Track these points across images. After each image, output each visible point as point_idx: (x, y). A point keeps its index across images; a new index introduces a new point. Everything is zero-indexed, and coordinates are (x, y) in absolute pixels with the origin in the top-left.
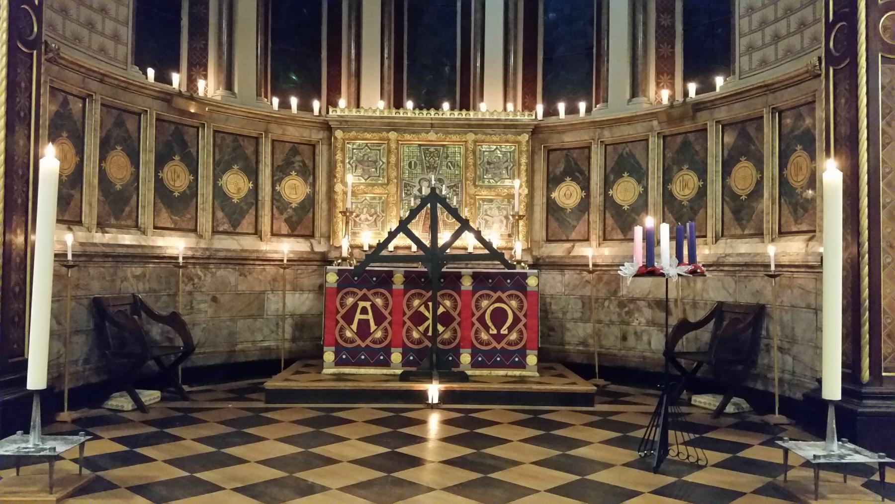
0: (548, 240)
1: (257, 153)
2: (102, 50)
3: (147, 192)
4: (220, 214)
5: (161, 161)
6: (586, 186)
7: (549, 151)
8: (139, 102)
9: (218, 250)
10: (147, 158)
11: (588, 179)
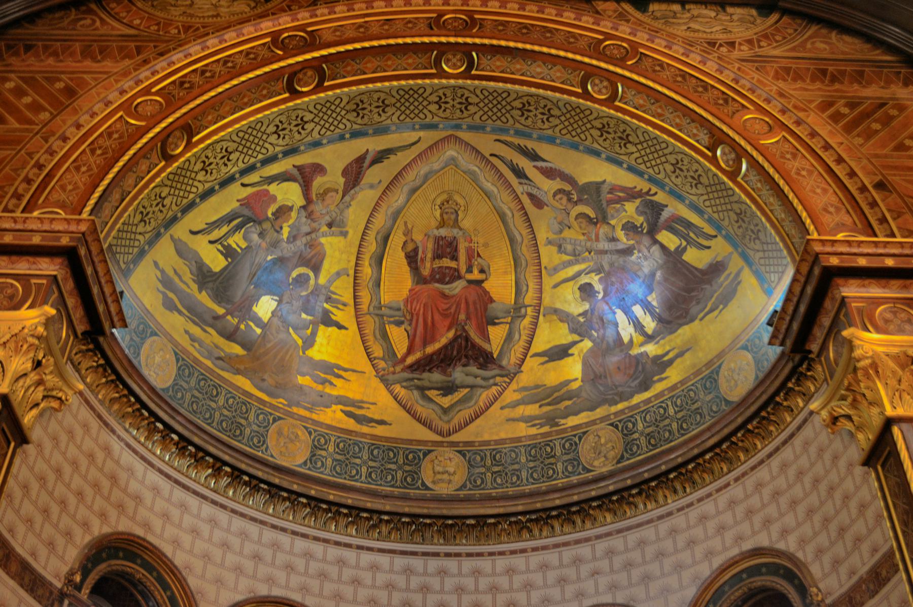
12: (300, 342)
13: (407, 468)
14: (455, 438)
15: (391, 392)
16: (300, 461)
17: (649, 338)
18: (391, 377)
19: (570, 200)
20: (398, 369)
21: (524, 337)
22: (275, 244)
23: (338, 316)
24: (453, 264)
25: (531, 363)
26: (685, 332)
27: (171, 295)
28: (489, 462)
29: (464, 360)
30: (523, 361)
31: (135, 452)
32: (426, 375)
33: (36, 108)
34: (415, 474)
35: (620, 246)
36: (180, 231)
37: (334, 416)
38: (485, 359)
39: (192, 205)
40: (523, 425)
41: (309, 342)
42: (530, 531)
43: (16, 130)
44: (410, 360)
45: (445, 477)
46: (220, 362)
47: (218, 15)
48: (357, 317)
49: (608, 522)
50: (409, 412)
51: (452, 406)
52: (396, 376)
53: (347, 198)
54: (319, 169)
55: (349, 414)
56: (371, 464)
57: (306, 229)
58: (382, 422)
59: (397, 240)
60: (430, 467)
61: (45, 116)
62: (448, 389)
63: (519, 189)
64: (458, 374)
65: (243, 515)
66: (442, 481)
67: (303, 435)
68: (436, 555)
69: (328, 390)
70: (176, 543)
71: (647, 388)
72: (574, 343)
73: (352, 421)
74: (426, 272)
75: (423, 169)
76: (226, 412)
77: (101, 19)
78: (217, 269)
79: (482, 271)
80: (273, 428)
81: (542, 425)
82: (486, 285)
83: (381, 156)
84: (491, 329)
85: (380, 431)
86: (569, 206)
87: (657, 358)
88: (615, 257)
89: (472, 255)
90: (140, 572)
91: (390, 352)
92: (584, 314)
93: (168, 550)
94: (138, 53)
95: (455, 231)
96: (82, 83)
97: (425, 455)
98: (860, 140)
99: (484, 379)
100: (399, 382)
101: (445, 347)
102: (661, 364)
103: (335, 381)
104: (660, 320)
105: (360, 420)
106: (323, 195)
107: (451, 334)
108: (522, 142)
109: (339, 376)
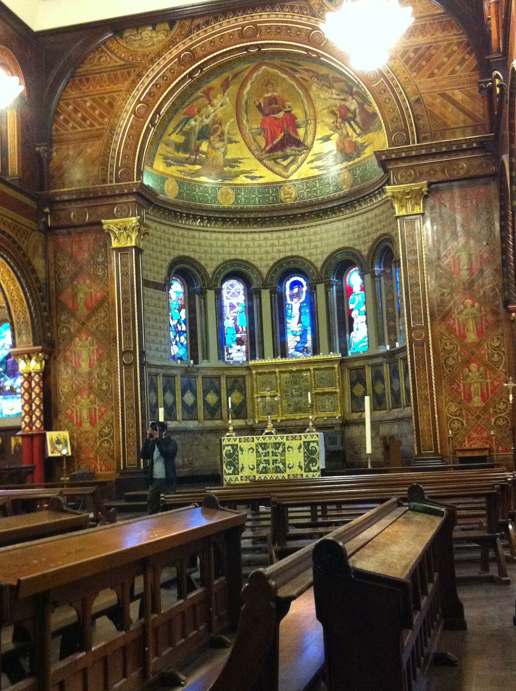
0: (353, 412)
1: (220, 384)
3: (179, 407)
4: (206, 412)
5: (183, 393)
6: (365, 387)
7: (350, 369)
8: (174, 372)
9: (206, 427)
10: (178, 393)
11: (365, 382)
13: (274, 195)
14: (290, 179)
15: (262, 163)
16: (232, 202)
17: (359, 135)
18: (261, 157)
19: (318, 79)
20: (264, 152)
21: (312, 133)
22: (202, 121)
23: (235, 138)
24: (277, 106)
25: (317, 144)
26: (370, 135)
27: (169, 161)
28: (305, 188)
29: (290, 144)
30: (313, 142)
31: (173, 226)
32: (275, 153)
33: (102, 116)
34: (277, 197)
35: (342, 97)
36: (165, 138)
37: (242, 180)
38: (298, 143)
40: (316, 170)
41: (225, 153)
42: (321, 217)
44: (267, 148)
45: (288, 196)
46: (194, 175)
47: (153, 45)
48: (242, 136)
49: (348, 213)
50: (271, 170)
51: (288, 164)
52: (263, 156)
53: (226, 94)
54: (210, 89)
55: (247, 177)
56: (260, 196)
57: (212, 111)
58: (261, 177)
59: (251, 103)
60: (282, 192)
61: (106, 120)
62: (285, 158)
64: (288, 151)
65: (215, 232)
66: (288, 198)
67: (231, 191)
68: (288, 230)
70: (194, 251)
71: (359, 157)
72: (332, 135)
73: (249, 179)
74: (267, 112)
75: (255, 75)
76: (200, 194)
77: (109, 56)
79: (289, 107)
80: (219, 193)
82: (292, 112)
83: (235, 76)
84: (298, 130)
85: (261, 181)
86: (318, 82)
87: (362, 144)
88: (340, 101)
89: (283, 102)
90: (185, 266)
92: (334, 123)
93: (192, 255)
94: (129, 76)
95: (275, 94)
96: (113, 98)
97: (280, 187)
98: (415, 74)
99: (299, 151)
100: (265, 158)
101: (281, 140)
102: (364, 147)
103: (239, 165)
104: (361, 129)
106: (215, 97)
107: (282, 134)
108: (292, 61)
109: (240, 162)
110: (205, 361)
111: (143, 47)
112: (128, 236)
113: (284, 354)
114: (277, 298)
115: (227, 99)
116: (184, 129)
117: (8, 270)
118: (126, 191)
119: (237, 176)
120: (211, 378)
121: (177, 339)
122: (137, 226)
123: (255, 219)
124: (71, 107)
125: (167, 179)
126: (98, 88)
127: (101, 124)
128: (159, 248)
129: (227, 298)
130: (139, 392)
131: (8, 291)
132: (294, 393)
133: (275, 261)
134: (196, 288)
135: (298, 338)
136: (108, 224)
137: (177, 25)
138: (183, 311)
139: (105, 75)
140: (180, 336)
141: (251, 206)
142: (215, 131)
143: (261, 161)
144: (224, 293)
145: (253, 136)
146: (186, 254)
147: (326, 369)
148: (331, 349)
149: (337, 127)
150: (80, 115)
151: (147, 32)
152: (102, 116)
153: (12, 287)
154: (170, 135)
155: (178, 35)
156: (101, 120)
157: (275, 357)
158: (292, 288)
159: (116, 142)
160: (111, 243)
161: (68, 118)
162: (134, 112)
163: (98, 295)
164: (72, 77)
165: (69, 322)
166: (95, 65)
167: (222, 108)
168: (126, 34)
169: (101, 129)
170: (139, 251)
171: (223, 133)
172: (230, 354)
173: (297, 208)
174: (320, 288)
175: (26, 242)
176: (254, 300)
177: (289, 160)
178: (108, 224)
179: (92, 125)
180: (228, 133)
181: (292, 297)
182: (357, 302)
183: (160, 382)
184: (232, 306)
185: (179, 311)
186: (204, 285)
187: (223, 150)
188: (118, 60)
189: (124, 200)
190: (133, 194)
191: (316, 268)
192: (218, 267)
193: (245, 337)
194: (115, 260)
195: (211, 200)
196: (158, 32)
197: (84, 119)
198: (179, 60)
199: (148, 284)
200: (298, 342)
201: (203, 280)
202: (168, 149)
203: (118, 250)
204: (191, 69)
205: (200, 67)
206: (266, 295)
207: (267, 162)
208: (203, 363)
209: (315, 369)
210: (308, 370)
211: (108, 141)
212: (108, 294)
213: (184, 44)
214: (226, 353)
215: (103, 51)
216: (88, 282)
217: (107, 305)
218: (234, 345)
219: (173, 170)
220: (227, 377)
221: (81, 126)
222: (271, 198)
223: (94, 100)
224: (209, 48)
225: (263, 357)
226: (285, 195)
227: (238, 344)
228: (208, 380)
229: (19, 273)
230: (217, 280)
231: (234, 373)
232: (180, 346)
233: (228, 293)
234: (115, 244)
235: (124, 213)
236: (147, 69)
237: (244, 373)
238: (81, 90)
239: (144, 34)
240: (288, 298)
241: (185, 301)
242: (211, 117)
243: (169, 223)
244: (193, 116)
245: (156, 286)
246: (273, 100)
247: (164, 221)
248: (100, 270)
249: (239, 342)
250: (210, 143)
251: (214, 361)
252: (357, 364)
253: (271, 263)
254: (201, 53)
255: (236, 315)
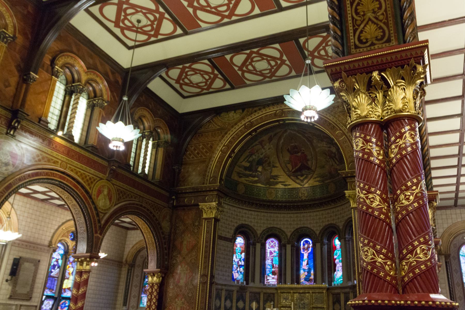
1: (260, 297)
2: (226, 279)
6: (340, 305)
10: (234, 301)
12: (269, 173)
15: (290, 178)
16: (273, 197)
20: (291, 173)
22: (259, 156)
24: (297, 150)
33: (206, 152)
37: (280, 186)
38: (309, 169)
39: (239, 158)
41: (271, 172)
43: (204, 159)
44: (293, 170)
47: (234, 119)
53: (271, 143)
55: (282, 185)
57: (264, 151)
58: (289, 185)
60: (300, 193)
61: (208, 154)
62: (302, 176)
63: (306, 135)
64: (304, 172)
69: (277, 180)
70: (251, 222)
75: (285, 135)
78: (248, 166)
81: (321, 182)
83: (275, 135)
85: (289, 187)
91: (289, 170)
93: (250, 224)
94: (221, 134)
95: (296, 144)
103: (277, 178)
105: (285, 185)
106: (265, 145)
110: (253, 283)
111: (229, 120)
112: (211, 212)
113: (298, 282)
114: (295, 250)
115: (272, 146)
116: (249, 160)
117: (147, 227)
118: (212, 189)
119: (277, 183)
120: (255, 293)
121: (238, 269)
122: (217, 207)
123: (285, 206)
124: (193, 148)
125: (239, 184)
126: (206, 139)
127: (205, 156)
128: (230, 219)
129: (269, 248)
130: (207, 299)
131: (147, 238)
132: (301, 306)
133: (295, 229)
134: (251, 241)
135: (306, 273)
136: (202, 205)
137: (246, 111)
138: (243, 254)
139: (210, 133)
140: (240, 268)
141: (284, 200)
142: (266, 161)
143: (289, 176)
144: (267, 245)
145: (286, 165)
146: (246, 223)
147: (318, 293)
148: (323, 281)
149: (327, 161)
150: (196, 152)
151: (232, 114)
152: (206, 152)
153: (149, 236)
154: (241, 162)
155: (246, 115)
156: (206, 154)
157: (292, 283)
158: (304, 245)
159: (211, 165)
160: (203, 215)
161: (191, 153)
162: (221, 150)
163: (194, 242)
164: (195, 134)
165: (177, 257)
166: (206, 129)
167: (269, 150)
168: (222, 115)
169: (205, 158)
170: (217, 220)
171: (270, 163)
172: (268, 280)
173: (307, 201)
174: (318, 245)
175: (159, 213)
176: (283, 250)
177: (304, 177)
178: (202, 205)
179: (201, 156)
180: (273, 163)
181: (304, 249)
182: (338, 255)
183: (224, 294)
184: (271, 253)
185: (241, 253)
186: (255, 240)
187: (270, 171)
188: (216, 126)
189: (211, 193)
190: (215, 190)
191: (316, 234)
192: (264, 231)
193: (277, 271)
194: (205, 224)
195: (263, 196)
196: (237, 114)
197: (198, 153)
198: (245, 126)
199: (221, 238)
200: (306, 276)
201: (255, 237)
202: (241, 169)
203: (206, 219)
204: (250, 130)
205: (255, 130)
206: (289, 247)
207: (293, 178)
208: (251, 284)
209: (313, 293)
210: (309, 293)
211: (208, 164)
212: (198, 242)
213: (248, 119)
214: (266, 279)
215: (211, 122)
216: (189, 235)
217: (197, 248)
218: (271, 275)
219: (243, 180)
220: (264, 293)
221: (196, 157)
222: (294, 196)
223: (203, 145)
224: (259, 121)
225: (285, 283)
226: (302, 194)
227: (273, 274)
228: (253, 294)
229: (152, 229)
230: (262, 238)
231: (269, 291)
232: (240, 273)
233: (269, 245)
234: (205, 216)
235: (210, 200)
236: (229, 130)
237: (274, 291)
238: (198, 140)
239: (230, 115)
240: (302, 250)
241: (245, 248)
242: (264, 154)
243: (238, 206)
244: (254, 154)
245: (226, 239)
246: (295, 147)
247: (235, 205)
248: (196, 229)
249: (274, 273)
250: (263, 167)
251: (257, 284)
252: (337, 291)
253: (293, 230)
254: (255, 123)
255: (272, 258)
